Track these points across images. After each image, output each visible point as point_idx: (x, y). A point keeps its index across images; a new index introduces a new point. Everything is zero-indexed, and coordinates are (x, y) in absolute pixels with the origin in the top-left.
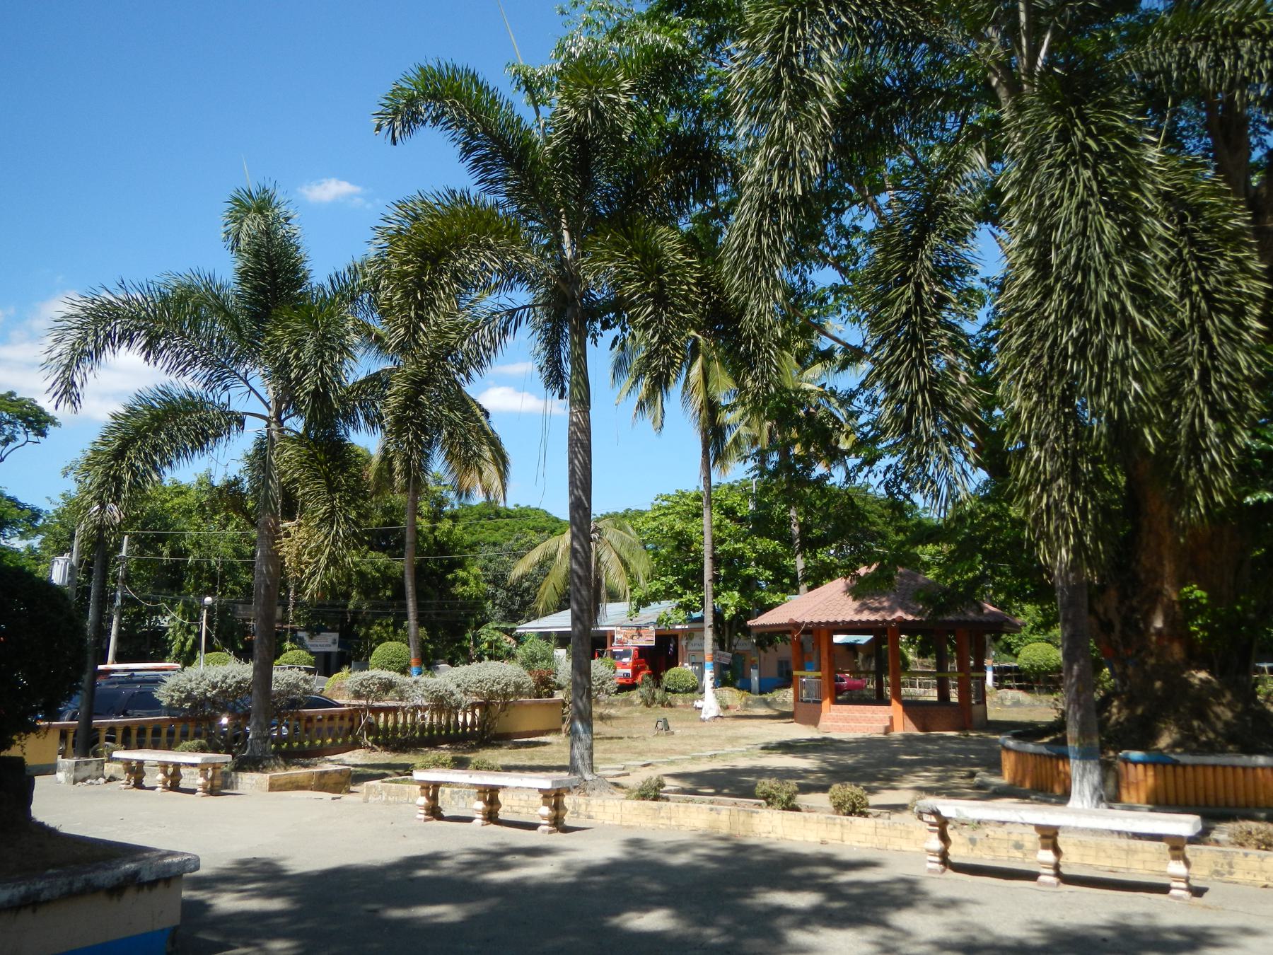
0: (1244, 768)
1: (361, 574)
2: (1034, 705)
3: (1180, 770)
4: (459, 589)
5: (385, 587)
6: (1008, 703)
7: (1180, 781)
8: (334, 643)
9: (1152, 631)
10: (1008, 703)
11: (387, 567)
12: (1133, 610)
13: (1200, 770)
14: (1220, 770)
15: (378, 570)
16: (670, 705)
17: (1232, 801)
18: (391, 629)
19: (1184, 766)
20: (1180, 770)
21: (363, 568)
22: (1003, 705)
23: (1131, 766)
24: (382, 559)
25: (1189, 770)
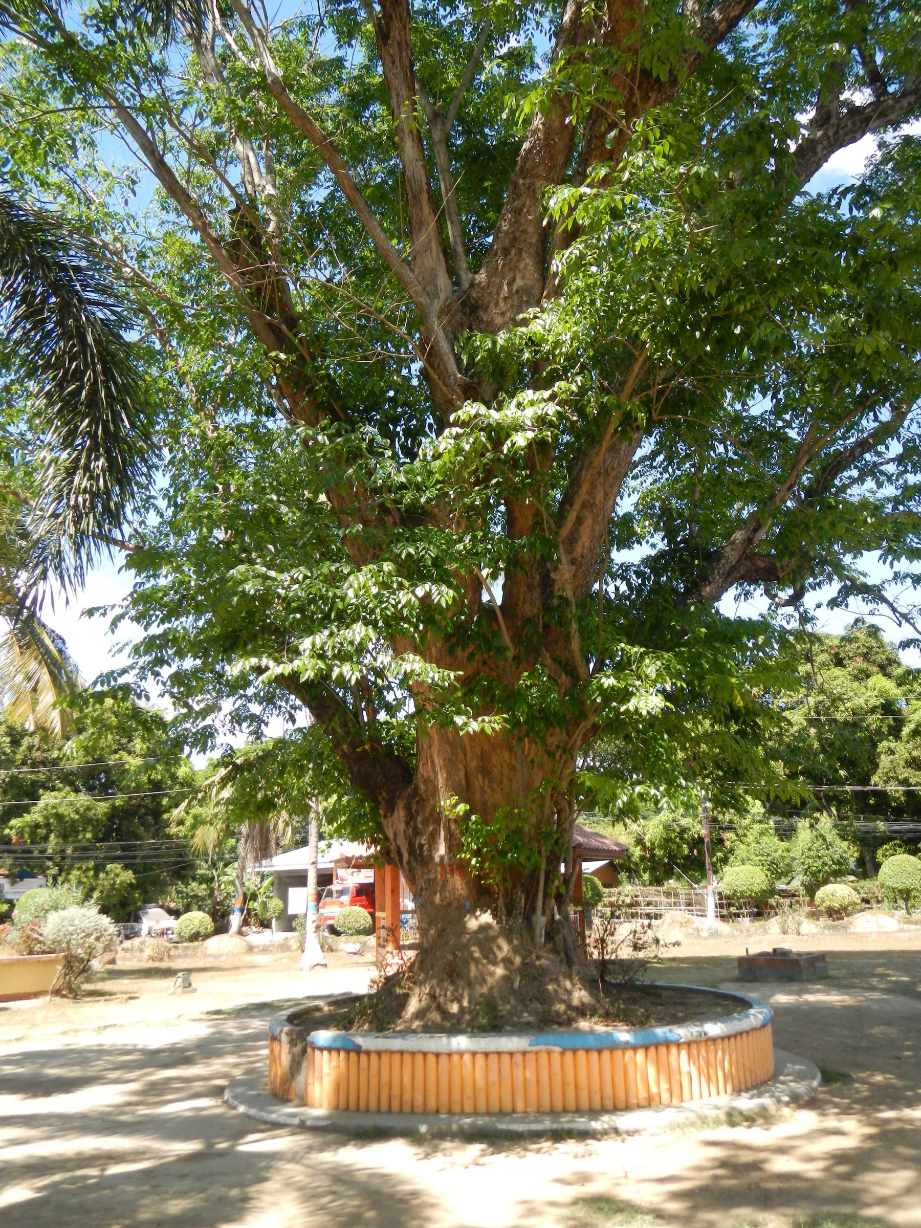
0: (437, 1055)
1: (59, 817)
2: (733, 936)
3: (363, 1058)
4: (173, 830)
5: (84, 830)
6: (705, 934)
7: (363, 1075)
9: (437, 859)
10: (705, 934)
11: (88, 809)
12: (417, 833)
13: (385, 1058)
14: (407, 1058)
15: (77, 812)
16: (331, 949)
17: (373, 1106)
18: (91, 873)
19: (368, 1053)
20: (363, 1058)
21: (61, 810)
23: (317, 1052)
24: (83, 799)
25: (374, 1057)
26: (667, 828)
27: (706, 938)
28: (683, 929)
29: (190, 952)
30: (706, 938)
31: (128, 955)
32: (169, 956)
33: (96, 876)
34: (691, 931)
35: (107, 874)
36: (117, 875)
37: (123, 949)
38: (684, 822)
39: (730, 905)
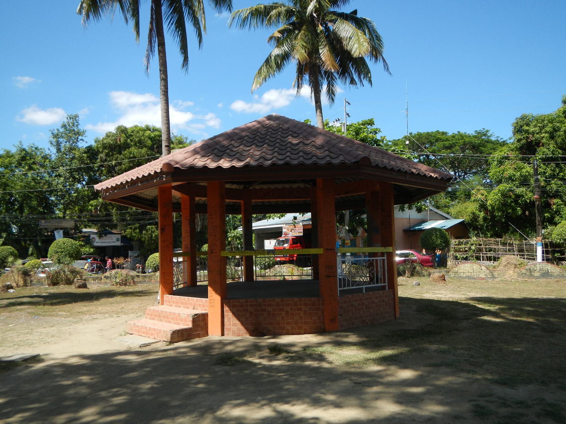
6: (537, 274)
8: (118, 240)
10: (537, 274)
18: (138, 231)
22: (531, 276)
26: (504, 195)
27: (538, 278)
28: (517, 270)
29: (147, 280)
30: (538, 278)
31: (108, 281)
32: (134, 282)
33: (141, 232)
34: (524, 271)
35: (147, 231)
36: (154, 232)
37: (105, 277)
38: (519, 191)
39: (554, 252)
